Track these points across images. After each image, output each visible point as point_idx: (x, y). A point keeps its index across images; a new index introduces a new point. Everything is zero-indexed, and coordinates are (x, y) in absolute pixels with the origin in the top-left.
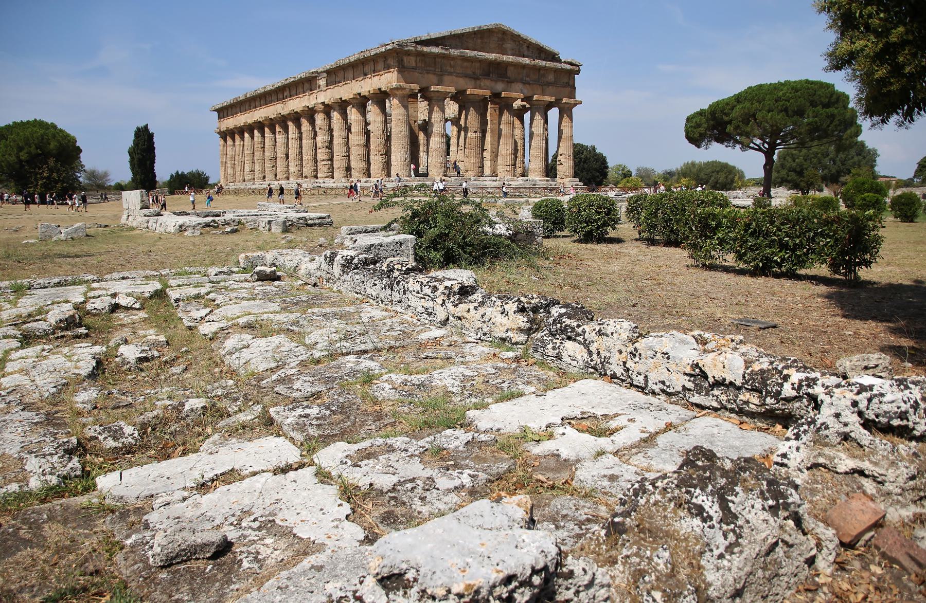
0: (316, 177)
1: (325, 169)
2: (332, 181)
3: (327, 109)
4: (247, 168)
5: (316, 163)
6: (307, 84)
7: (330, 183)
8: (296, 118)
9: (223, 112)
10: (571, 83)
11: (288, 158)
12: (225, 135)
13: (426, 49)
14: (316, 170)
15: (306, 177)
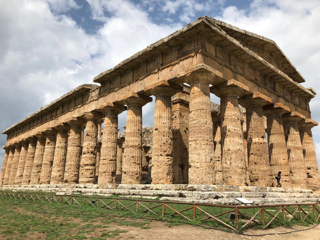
0: (77, 181)
1: (88, 174)
2: (96, 186)
3: (98, 116)
4: (18, 174)
5: (78, 168)
6: (80, 96)
7: (91, 189)
8: (64, 130)
9: (11, 133)
10: (308, 108)
11: (52, 165)
12: (10, 149)
13: (229, 37)
14: (78, 176)
15: (66, 182)
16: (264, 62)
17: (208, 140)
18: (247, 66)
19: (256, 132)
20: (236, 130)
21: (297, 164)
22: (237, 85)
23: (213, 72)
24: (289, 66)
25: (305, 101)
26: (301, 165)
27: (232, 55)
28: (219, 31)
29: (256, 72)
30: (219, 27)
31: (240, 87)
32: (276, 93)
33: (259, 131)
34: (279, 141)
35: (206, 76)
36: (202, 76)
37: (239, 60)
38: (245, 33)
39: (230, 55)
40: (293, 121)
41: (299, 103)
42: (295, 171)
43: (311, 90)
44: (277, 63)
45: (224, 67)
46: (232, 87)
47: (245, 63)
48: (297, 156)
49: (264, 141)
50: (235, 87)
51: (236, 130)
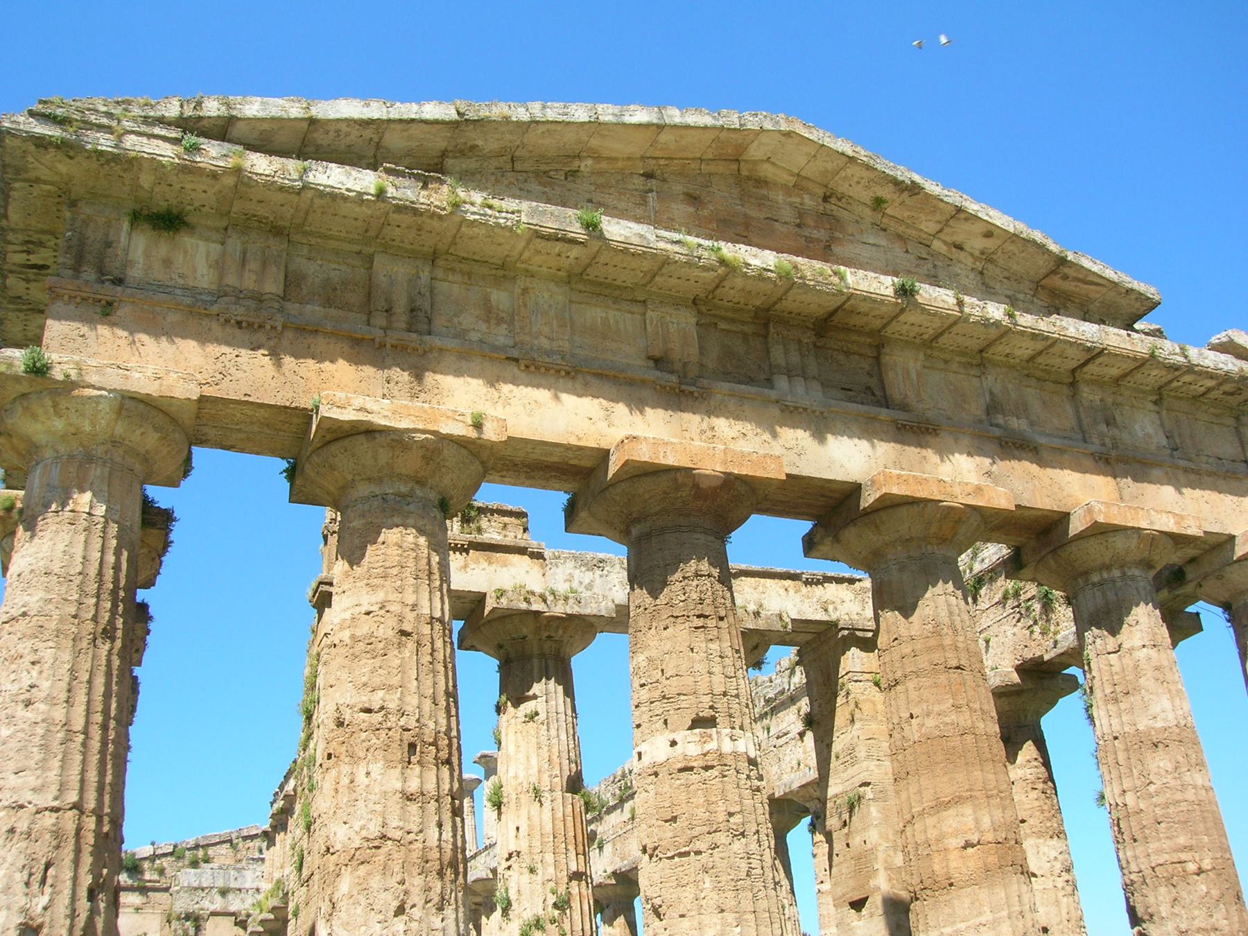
16: (662, 245)
17: (22, 807)
18: (548, 296)
19: (657, 694)
20: (376, 707)
21: (1160, 851)
22: (370, 418)
23: (93, 379)
24: (988, 235)
25: (1230, 421)
26: (1183, 856)
27: (378, 259)
28: (166, 152)
29: (649, 314)
30: (163, 132)
31: (403, 424)
32: (884, 414)
33: (672, 687)
34: (930, 722)
35: (58, 414)
36: (35, 417)
37: (469, 275)
38: (455, 117)
39: (370, 260)
40: (1108, 567)
41: (1164, 442)
42: (1151, 900)
43: (1229, 348)
44: (901, 238)
45: (289, 334)
46: (346, 442)
47: (522, 282)
48: (1157, 793)
49: (712, 746)
50: (362, 438)
51: (376, 707)
